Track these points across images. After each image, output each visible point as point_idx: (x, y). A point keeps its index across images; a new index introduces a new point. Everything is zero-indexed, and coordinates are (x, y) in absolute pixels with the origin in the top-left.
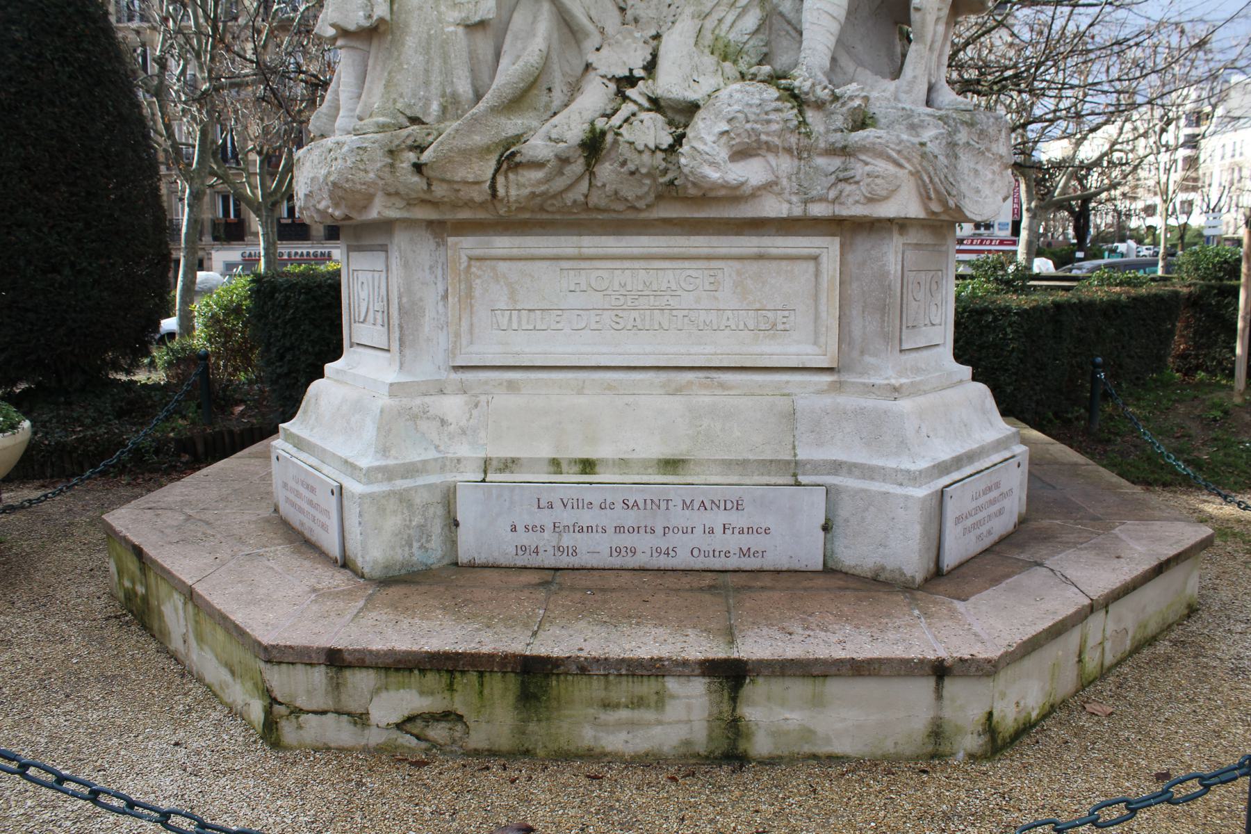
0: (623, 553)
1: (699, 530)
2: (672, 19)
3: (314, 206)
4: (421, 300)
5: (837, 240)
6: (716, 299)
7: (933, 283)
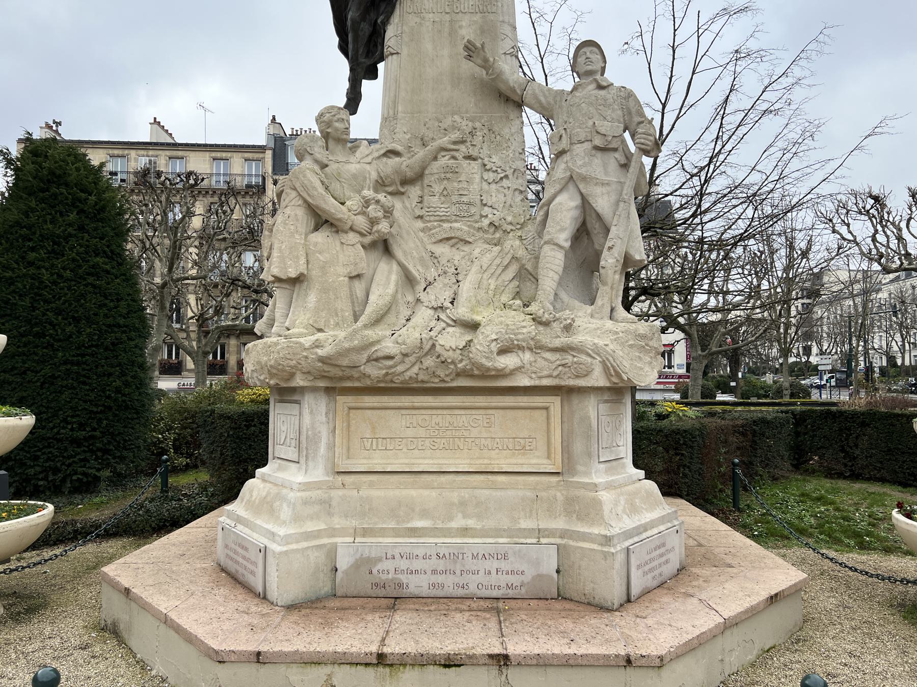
0: (437, 587)
1: (482, 572)
2: (465, 273)
3: (257, 377)
4: (319, 432)
5: (560, 398)
6: (490, 432)
7: (617, 422)
